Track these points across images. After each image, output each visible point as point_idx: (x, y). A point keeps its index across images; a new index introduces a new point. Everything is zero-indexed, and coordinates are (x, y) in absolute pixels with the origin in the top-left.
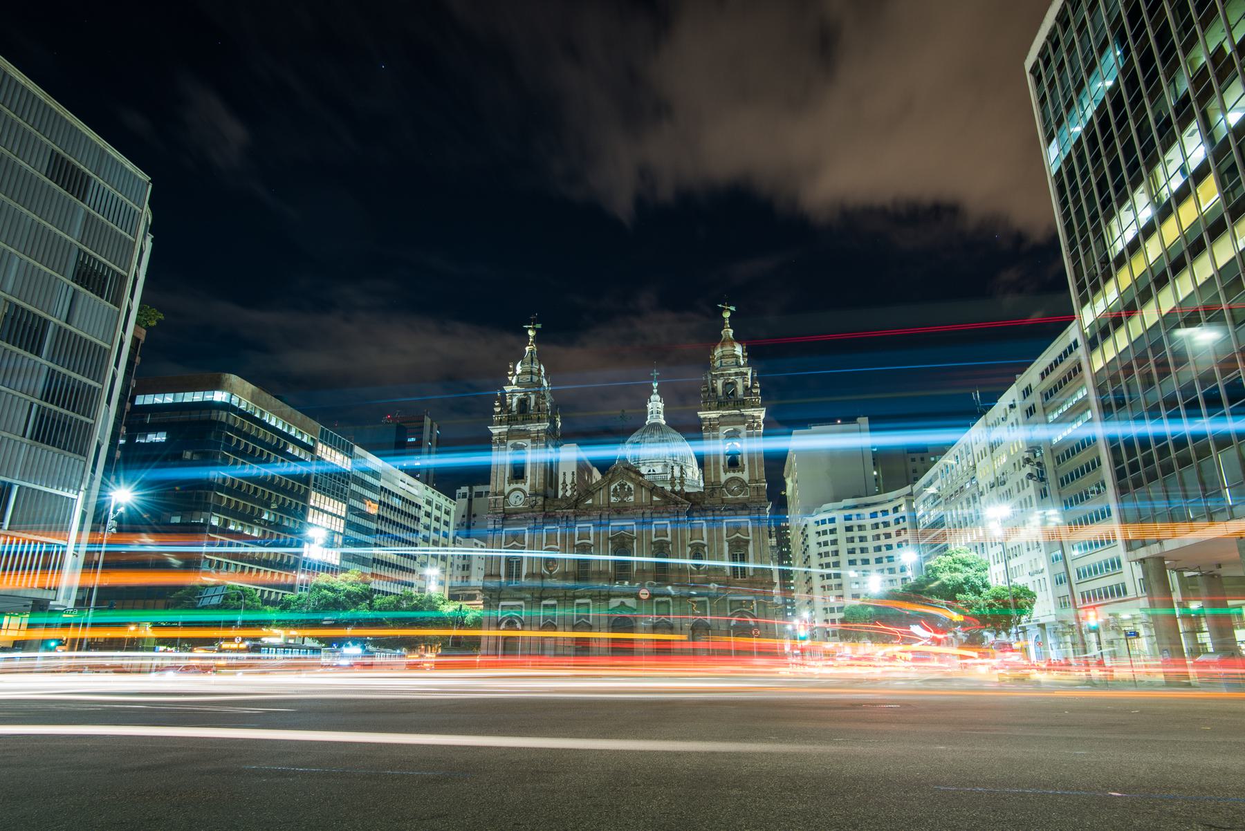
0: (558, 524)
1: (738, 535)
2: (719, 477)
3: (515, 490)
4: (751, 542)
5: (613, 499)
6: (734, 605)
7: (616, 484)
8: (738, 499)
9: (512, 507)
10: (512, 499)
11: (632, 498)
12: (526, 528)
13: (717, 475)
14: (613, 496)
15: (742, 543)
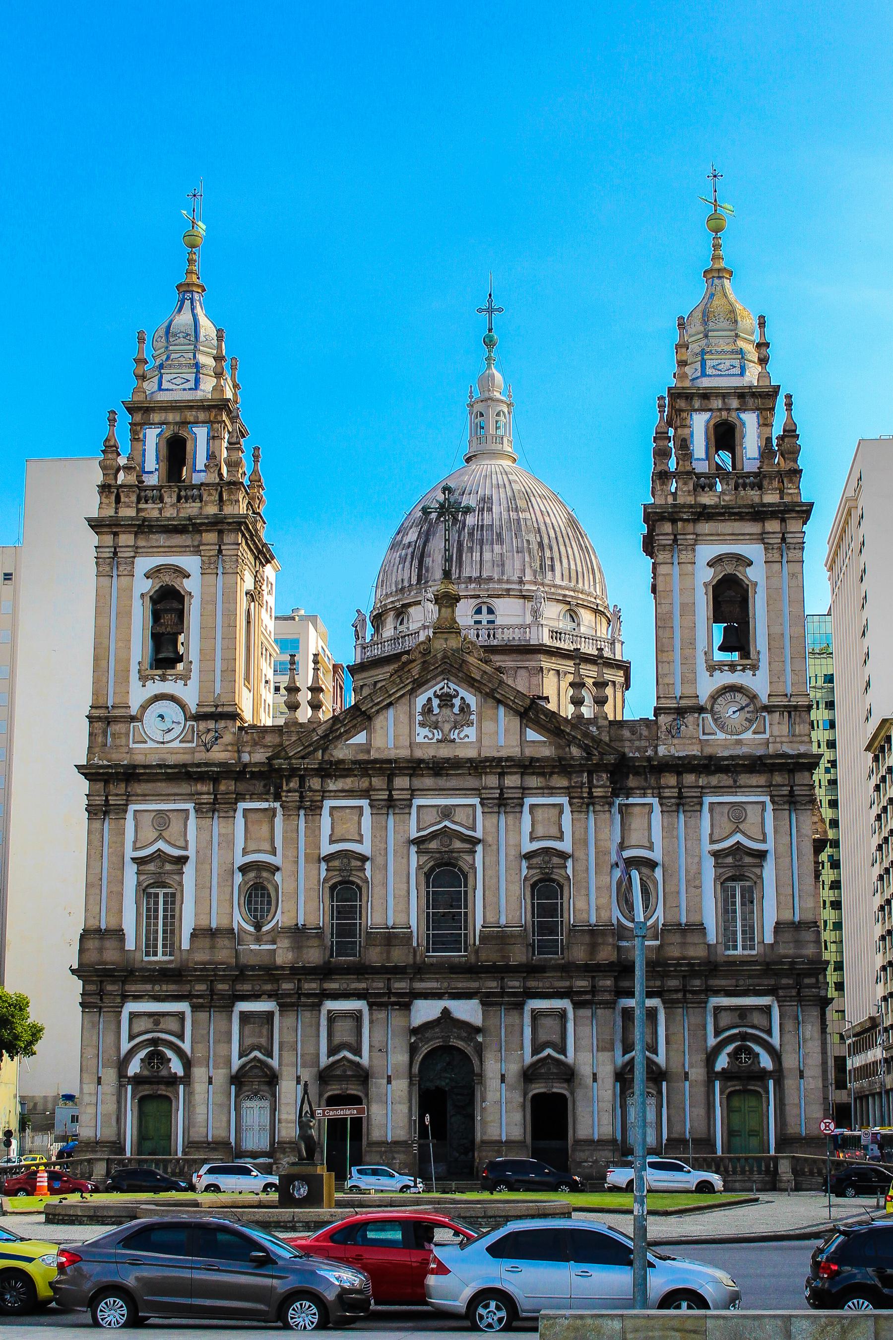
0: (277, 797)
3: (158, 698)
5: (422, 734)
7: (430, 693)
8: (739, 742)
9: (150, 744)
10: (151, 725)
11: (470, 733)
12: (190, 806)
13: (690, 679)
14: (422, 725)
15: (748, 860)
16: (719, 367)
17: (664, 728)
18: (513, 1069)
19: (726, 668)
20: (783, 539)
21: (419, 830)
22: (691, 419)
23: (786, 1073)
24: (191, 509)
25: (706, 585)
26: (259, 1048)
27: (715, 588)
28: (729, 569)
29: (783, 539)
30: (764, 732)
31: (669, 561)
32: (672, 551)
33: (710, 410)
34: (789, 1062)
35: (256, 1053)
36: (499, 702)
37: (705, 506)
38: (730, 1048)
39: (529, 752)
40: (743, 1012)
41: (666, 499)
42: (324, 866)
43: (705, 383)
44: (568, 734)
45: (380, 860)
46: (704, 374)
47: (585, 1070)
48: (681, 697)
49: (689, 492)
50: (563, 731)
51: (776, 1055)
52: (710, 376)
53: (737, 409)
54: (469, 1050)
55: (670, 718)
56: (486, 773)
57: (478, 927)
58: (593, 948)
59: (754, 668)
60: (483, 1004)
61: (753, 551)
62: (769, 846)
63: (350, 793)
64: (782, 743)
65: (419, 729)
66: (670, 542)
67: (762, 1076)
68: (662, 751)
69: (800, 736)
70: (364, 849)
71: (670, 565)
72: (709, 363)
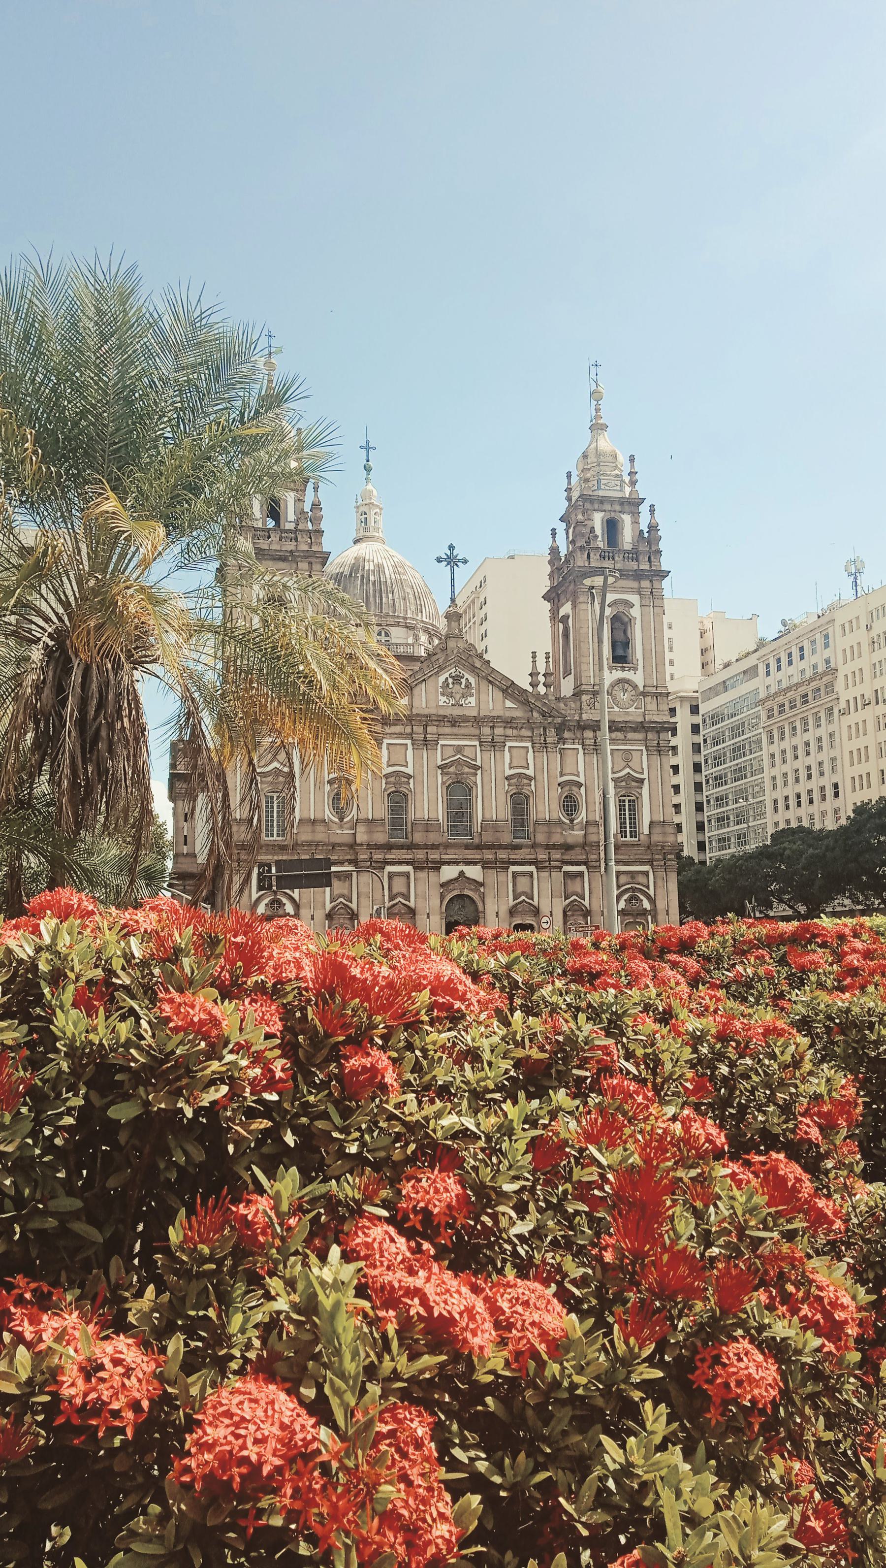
1: (628, 770)
4: (646, 782)
6: (623, 879)
11: (472, 700)
14: (443, 694)
18: (504, 910)
21: (443, 760)
23: (659, 911)
24: (290, 546)
26: (343, 896)
34: (661, 905)
35: (341, 900)
38: (626, 897)
39: (508, 714)
40: (632, 874)
42: (384, 781)
43: (601, 493)
45: (418, 778)
46: (599, 488)
47: (545, 909)
51: (653, 901)
54: (476, 897)
57: (480, 821)
58: (550, 834)
59: (635, 669)
60: (483, 868)
61: (634, 598)
62: (645, 776)
63: (400, 735)
65: (440, 697)
67: (644, 913)
68: (585, 717)
70: (409, 770)
72: (603, 482)
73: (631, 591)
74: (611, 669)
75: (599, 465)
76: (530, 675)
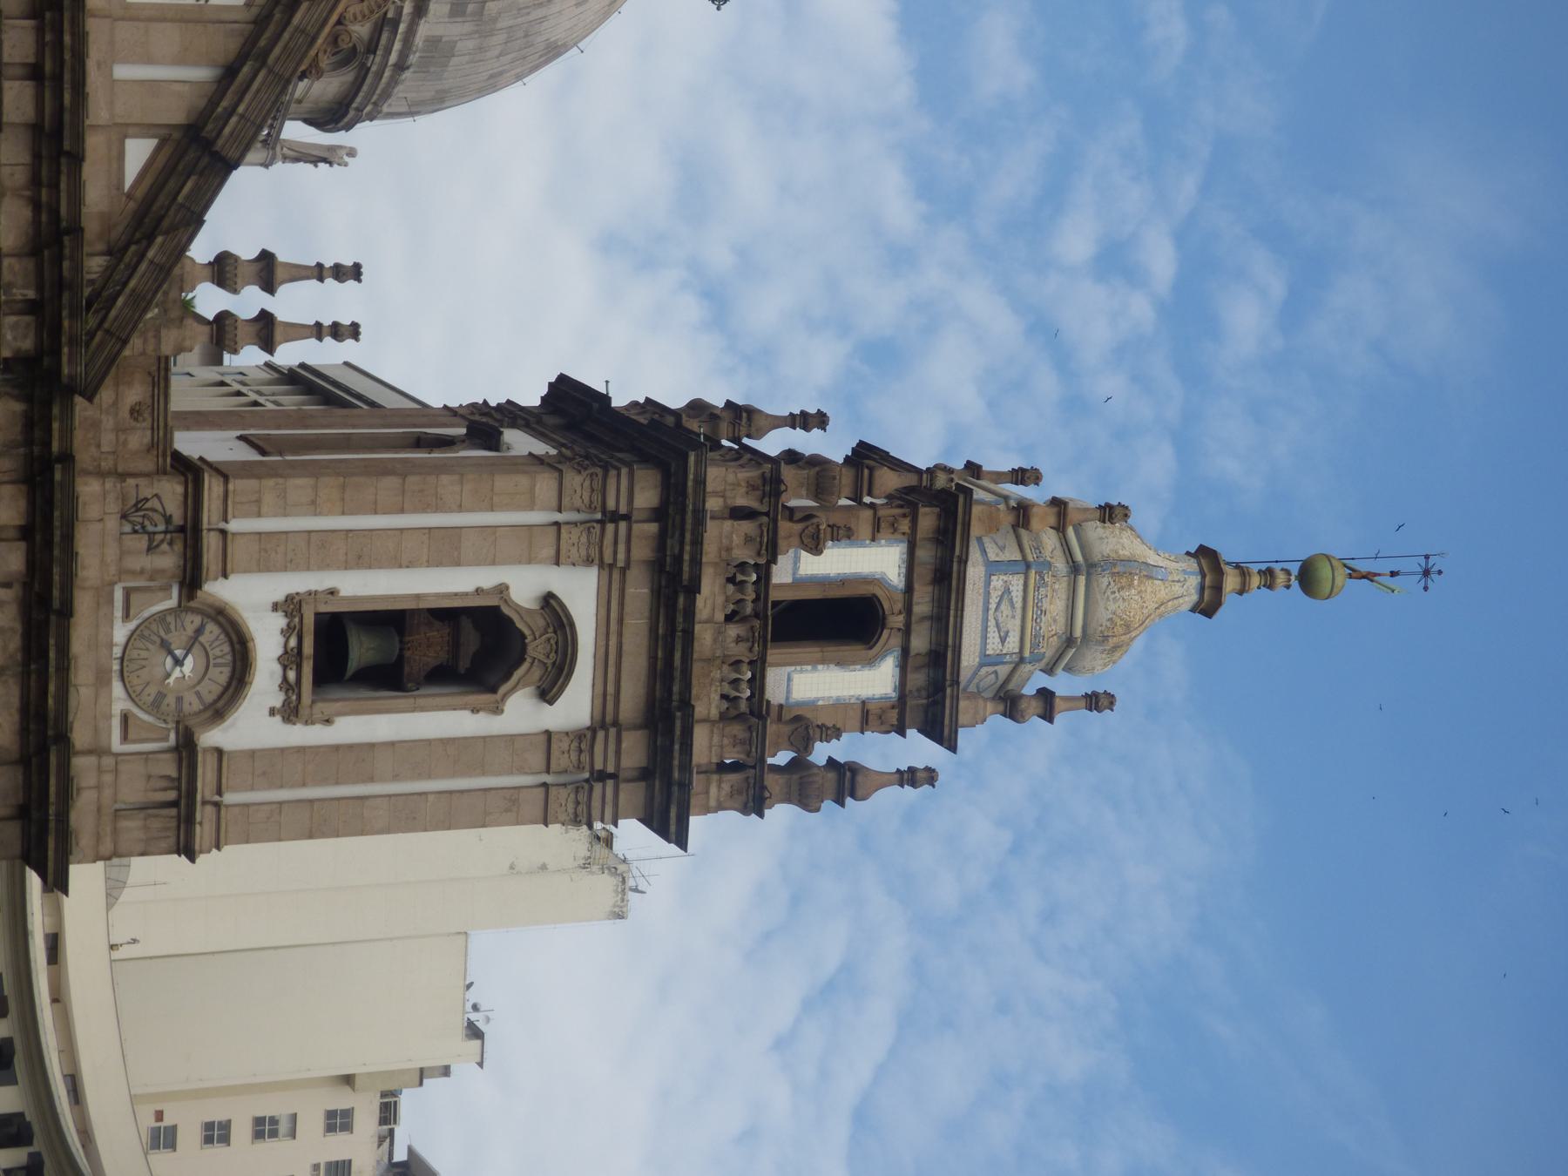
2: (264, 564)
8: (102, 680)
16: (1005, 607)
17: (146, 492)
19: (293, 642)
20: (602, 776)
22: (890, 543)
25: (502, 589)
27: (496, 609)
28: (537, 648)
29: (602, 776)
30: (125, 738)
31: (565, 501)
32: (591, 508)
33: (909, 588)
36: (230, 72)
37: (694, 589)
39: (95, 144)
41: (715, 494)
44: (142, 256)
48: (223, 532)
49: (729, 549)
50: (150, 238)
52: (988, 583)
53: (905, 651)
55: (174, 507)
56: (40, 31)
59: (290, 712)
64: (99, 787)
66: (611, 504)
68: (88, 489)
69: (115, 831)
71: (554, 503)
73: (606, 697)
74: (291, 606)
75: (1075, 569)
76: (266, 258)
